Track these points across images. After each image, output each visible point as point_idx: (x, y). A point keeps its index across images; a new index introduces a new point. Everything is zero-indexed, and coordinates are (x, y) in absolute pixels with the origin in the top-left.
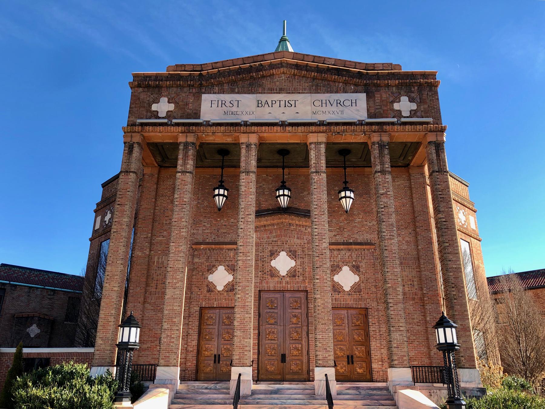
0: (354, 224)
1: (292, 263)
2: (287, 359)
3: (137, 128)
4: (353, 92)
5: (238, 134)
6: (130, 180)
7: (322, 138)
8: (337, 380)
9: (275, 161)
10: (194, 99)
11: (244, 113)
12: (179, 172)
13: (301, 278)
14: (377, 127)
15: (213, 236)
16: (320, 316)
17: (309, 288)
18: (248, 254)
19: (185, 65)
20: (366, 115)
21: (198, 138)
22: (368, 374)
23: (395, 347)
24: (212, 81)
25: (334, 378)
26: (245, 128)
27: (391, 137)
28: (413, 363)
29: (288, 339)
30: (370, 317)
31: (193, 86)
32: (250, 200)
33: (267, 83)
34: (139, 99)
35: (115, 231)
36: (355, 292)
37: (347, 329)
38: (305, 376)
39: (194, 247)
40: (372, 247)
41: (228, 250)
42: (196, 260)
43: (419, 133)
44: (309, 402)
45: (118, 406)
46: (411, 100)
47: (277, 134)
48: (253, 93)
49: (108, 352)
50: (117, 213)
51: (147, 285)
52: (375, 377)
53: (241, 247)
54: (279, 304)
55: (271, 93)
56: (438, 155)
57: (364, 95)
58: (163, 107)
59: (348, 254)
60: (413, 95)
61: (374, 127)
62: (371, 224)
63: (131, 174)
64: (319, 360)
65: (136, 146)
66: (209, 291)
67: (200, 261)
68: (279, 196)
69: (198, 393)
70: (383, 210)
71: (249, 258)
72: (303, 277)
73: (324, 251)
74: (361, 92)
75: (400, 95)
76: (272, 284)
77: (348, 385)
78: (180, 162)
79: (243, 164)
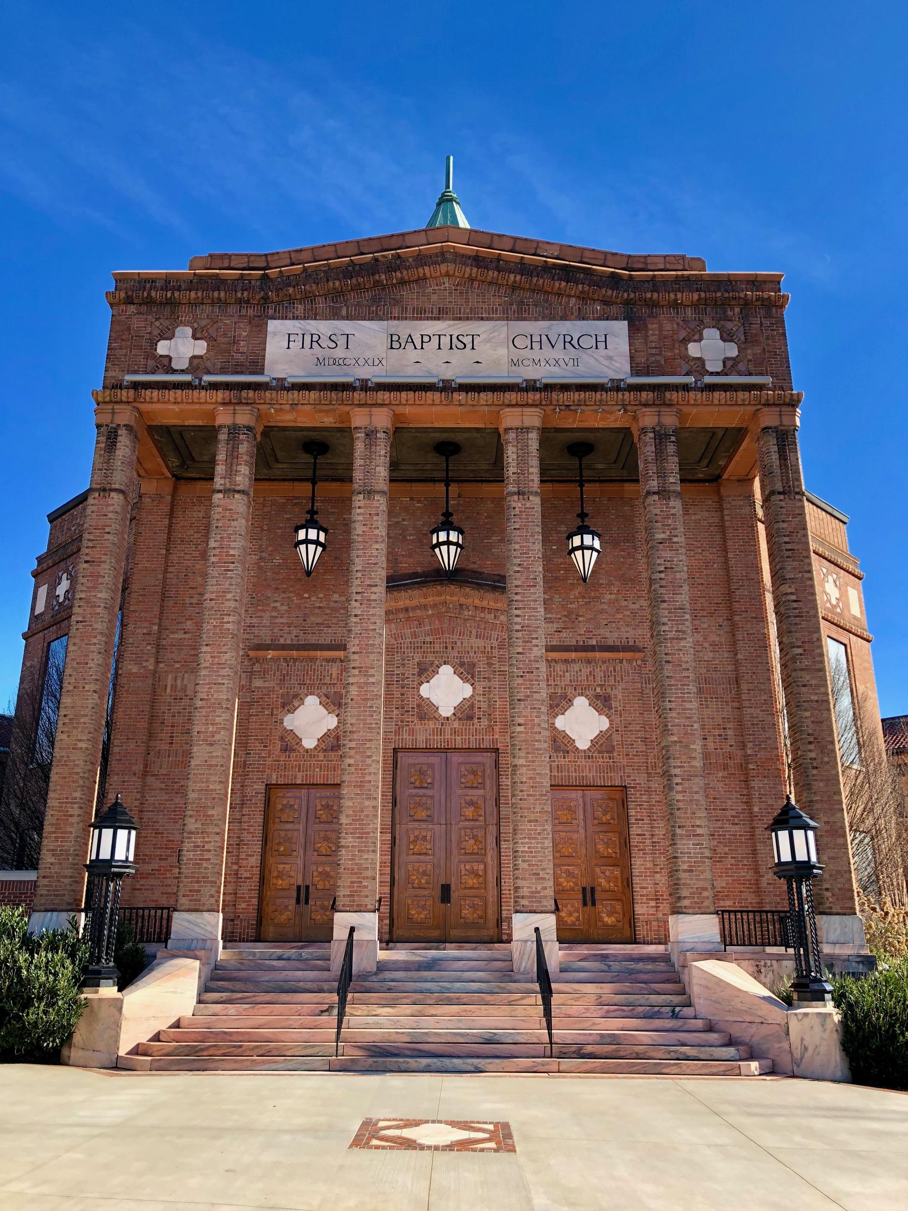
0: (601, 607)
1: (467, 691)
2: (454, 895)
3: (124, 394)
4: (599, 319)
5: (347, 408)
6: (111, 508)
7: (532, 418)
8: (560, 941)
9: (428, 467)
10: (251, 331)
11: (361, 362)
12: (219, 491)
13: (485, 722)
14: (651, 395)
15: (295, 632)
16: (524, 804)
17: (502, 742)
18: (371, 672)
19: (230, 257)
20: (627, 368)
21: (259, 417)
22: (627, 926)
23: (685, 871)
24: (291, 290)
25: (554, 937)
26: (363, 394)
27: (682, 416)
28: (722, 903)
29: (455, 852)
30: (631, 805)
31: (248, 302)
32: (375, 553)
33: (410, 296)
34: (129, 329)
35: (80, 619)
36: (599, 752)
37: (582, 831)
38: (492, 932)
39: (252, 654)
40: (638, 655)
41: (328, 661)
42: (258, 683)
43: (742, 408)
44: (500, 987)
45: (89, 996)
46: (726, 337)
47: (434, 409)
48: (381, 319)
49: (67, 881)
50: (84, 580)
51: (151, 735)
52: (642, 932)
53: (356, 657)
54: (437, 776)
55: (421, 319)
56: (783, 457)
57: (621, 327)
58: (183, 347)
59: (586, 670)
60: (729, 325)
61: (644, 394)
62: (637, 606)
63: (113, 494)
64: (523, 897)
65: (122, 432)
66: (286, 749)
67: (266, 684)
68: (439, 544)
69: (260, 968)
70: (662, 575)
71: (371, 680)
72: (490, 720)
73: (535, 665)
74: (616, 319)
75: (702, 325)
76: (422, 735)
77: (583, 950)
78: (220, 469)
79: (358, 475)
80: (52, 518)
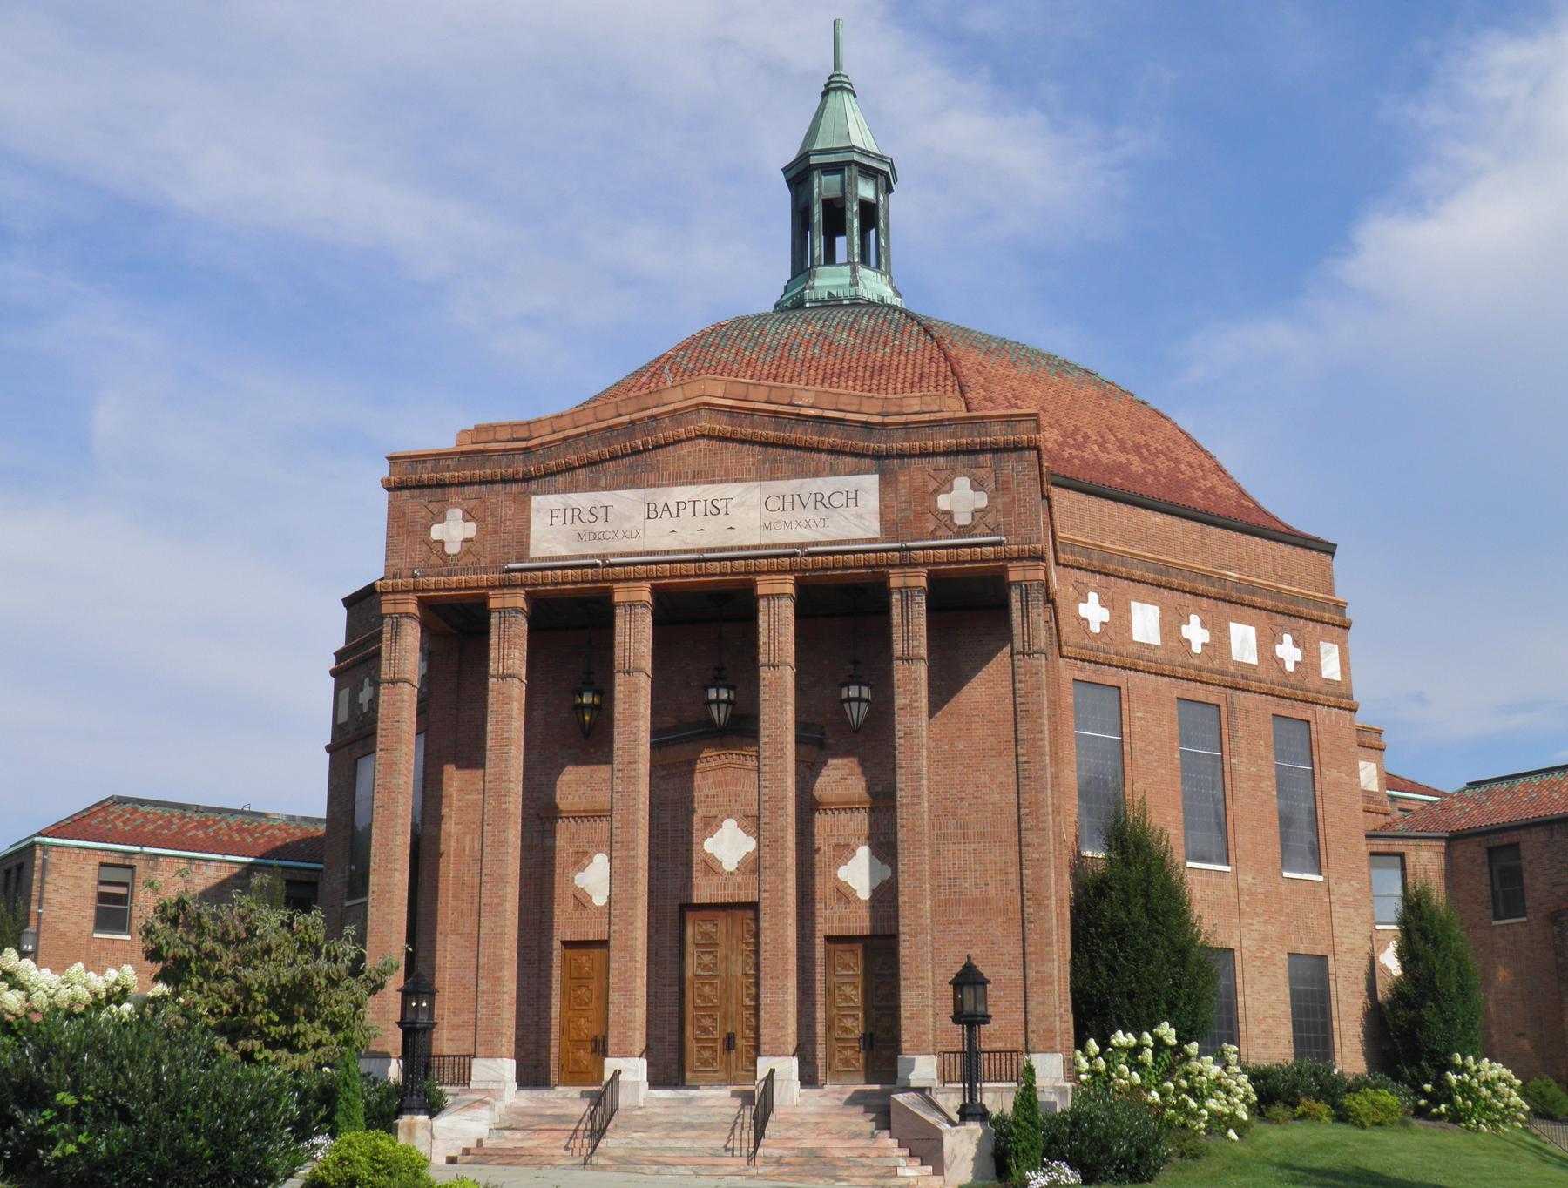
4: (850, 474)
11: (620, 535)
19: (493, 428)
20: (877, 526)
46: (977, 486)
57: (871, 481)
58: (454, 531)
66: (576, 907)
74: (867, 473)
79: (618, 652)
80: (349, 602)
